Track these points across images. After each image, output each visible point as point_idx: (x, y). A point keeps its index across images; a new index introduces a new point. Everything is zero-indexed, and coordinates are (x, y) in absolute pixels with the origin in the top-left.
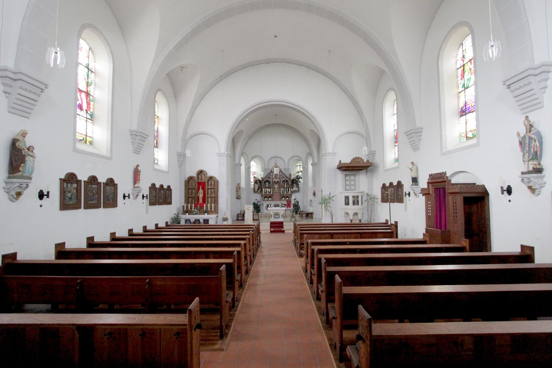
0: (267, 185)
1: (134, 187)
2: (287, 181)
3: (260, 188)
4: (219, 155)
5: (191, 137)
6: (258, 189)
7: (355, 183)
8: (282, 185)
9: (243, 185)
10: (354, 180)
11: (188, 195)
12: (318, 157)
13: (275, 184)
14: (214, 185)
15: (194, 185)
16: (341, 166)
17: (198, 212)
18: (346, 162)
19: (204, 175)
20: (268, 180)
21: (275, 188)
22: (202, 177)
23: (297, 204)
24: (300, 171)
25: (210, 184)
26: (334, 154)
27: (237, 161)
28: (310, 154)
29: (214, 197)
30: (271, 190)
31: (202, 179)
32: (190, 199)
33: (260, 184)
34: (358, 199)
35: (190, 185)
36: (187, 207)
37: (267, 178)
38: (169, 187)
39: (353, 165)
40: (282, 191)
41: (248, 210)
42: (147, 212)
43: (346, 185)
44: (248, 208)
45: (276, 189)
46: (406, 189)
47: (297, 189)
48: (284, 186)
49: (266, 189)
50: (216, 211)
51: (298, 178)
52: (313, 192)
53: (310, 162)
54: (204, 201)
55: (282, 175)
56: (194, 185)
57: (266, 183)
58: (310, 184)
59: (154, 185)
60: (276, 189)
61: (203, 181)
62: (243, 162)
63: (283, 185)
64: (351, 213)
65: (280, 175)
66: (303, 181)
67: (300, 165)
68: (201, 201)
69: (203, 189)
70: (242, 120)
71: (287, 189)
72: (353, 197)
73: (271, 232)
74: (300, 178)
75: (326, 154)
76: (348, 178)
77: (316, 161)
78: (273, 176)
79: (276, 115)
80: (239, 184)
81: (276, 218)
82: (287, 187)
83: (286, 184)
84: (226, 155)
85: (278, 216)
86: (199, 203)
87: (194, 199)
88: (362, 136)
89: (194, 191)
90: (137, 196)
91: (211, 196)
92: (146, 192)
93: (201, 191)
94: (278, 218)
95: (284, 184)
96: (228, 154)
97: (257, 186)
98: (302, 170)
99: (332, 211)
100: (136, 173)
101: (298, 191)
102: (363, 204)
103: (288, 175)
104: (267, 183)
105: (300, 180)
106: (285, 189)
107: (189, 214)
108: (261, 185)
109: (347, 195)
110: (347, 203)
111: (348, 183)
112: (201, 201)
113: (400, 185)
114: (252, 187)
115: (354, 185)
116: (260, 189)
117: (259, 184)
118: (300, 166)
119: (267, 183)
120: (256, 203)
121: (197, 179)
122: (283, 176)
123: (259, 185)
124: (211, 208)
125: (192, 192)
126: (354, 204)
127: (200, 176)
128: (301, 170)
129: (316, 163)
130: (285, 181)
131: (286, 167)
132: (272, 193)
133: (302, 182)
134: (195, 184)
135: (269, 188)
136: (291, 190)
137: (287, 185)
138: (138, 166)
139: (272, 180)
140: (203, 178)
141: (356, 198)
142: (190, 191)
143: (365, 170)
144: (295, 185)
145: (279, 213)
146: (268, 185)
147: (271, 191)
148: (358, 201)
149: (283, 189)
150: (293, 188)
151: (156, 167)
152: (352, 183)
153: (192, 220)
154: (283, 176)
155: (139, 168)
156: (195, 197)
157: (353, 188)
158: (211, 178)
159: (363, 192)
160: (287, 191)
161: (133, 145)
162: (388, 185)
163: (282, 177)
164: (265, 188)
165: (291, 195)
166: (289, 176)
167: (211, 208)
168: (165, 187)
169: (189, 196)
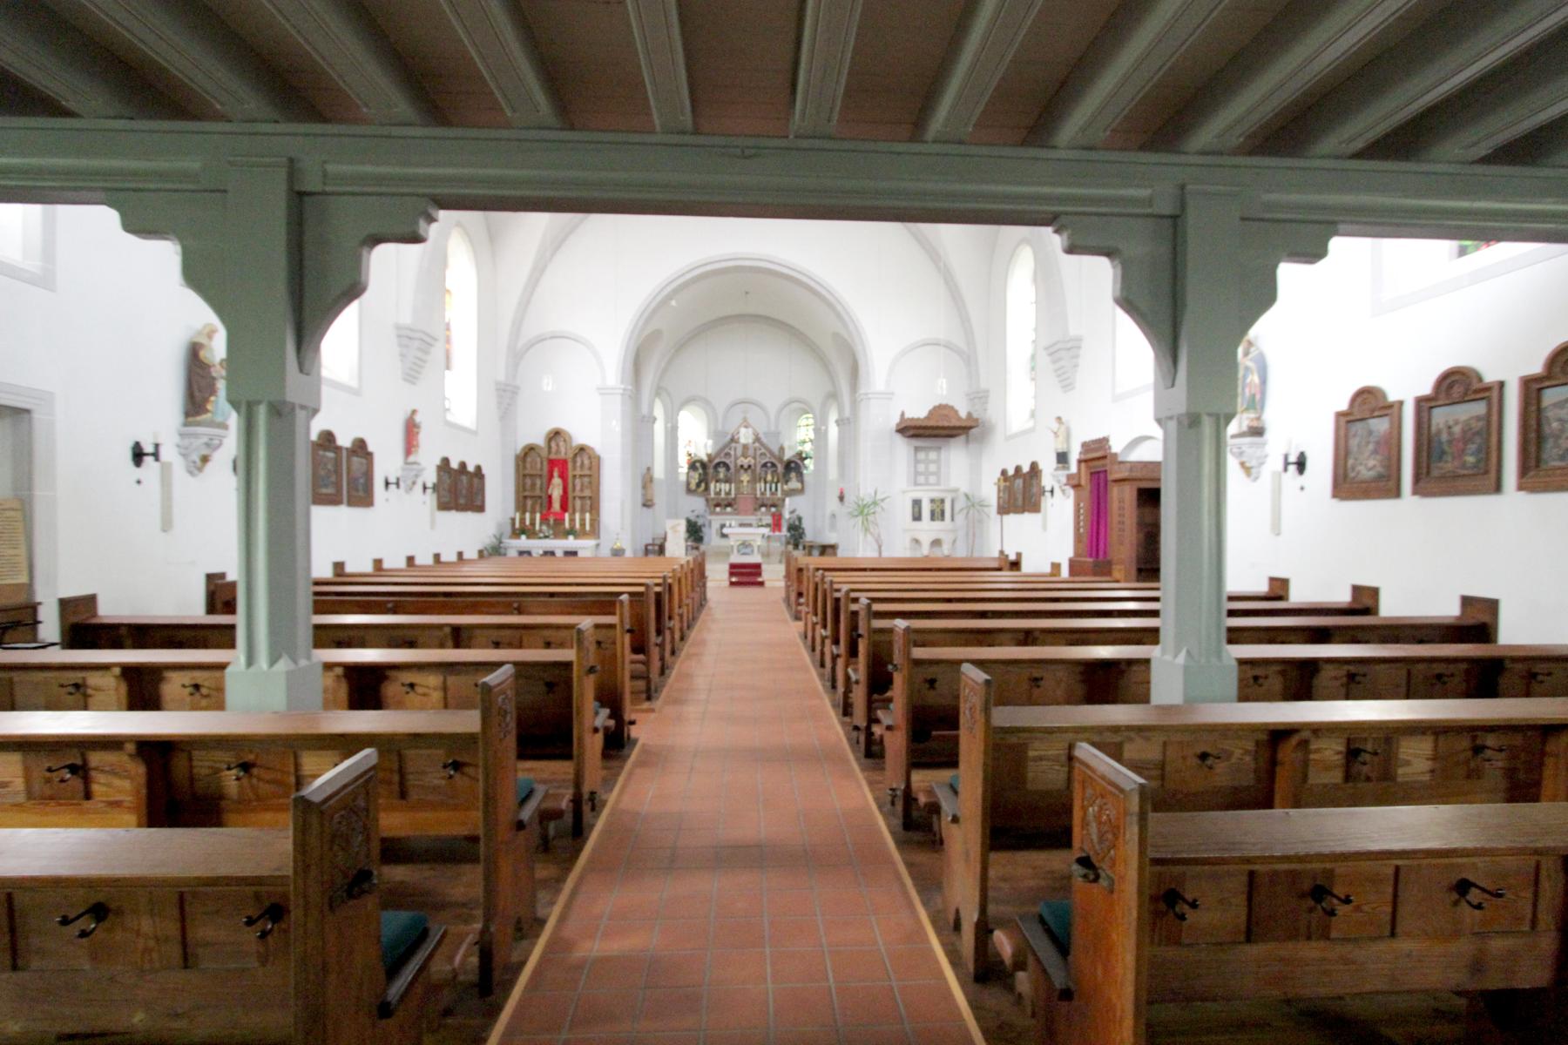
1: (406, 463)
2: (773, 465)
3: (704, 480)
4: (603, 391)
5: (531, 345)
6: (698, 485)
7: (939, 468)
9: (659, 472)
10: (937, 461)
11: (525, 490)
12: (855, 404)
13: (742, 471)
14: (590, 468)
15: (539, 466)
16: (903, 425)
17: (551, 532)
18: (916, 417)
19: (565, 441)
20: (723, 460)
21: (742, 482)
22: (558, 445)
23: (797, 523)
25: (578, 464)
26: (888, 395)
27: (645, 410)
28: (833, 396)
29: (590, 498)
31: (558, 451)
32: (529, 502)
33: (705, 471)
34: (943, 506)
35: (528, 466)
36: (522, 520)
37: (722, 455)
38: (478, 468)
39: (932, 423)
40: (760, 489)
41: (676, 531)
42: (433, 524)
43: (917, 473)
44: (674, 528)
45: (745, 484)
46: (1047, 480)
47: (798, 485)
48: (766, 474)
49: (718, 484)
50: (595, 532)
51: (801, 457)
52: (838, 494)
53: (833, 416)
54: (564, 507)
56: (538, 466)
58: (833, 472)
59: (446, 461)
60: (745, 484)
61: (562, 456)
62: (659, 412)
63: (763, 475)
64: (926, 540)
65: (755, 450)
66: (816, 465)
68: (556, 506)
69: (563, 476)
70: (659, 306)
71: (774, 486)
72: (932, 501)
73: (732, 584)
74: (806, 458)
75: (870, 396)
76: (922, 455)
77: (847, 413)
79: (747, 293)
80: (649, 469)
83: (769, 472)
84: (621, 391)
85: (748, 550)
86: (552, 510)
87: (539, 501)
88: (959, 352)
89: (538, 482)
90: (414, 483)
91: (582, 495)
92: (431, 477)
93: (557, 481)
96: (624, 390)
97: (695, 477)
99: (879, 535)
100: (411, 430)
101: (801, 491)
102: (956, 517)
103: (776, 450)
104: (722, 470)
105: (807, 462)
107: (528, 537)
108: (705, 474)
109: (917, 495)
110: (917, 517)
111: (921, 467)
112: (556, 506)
113: (1035, 470)
114: (683, 478)
115: (937, 474)
117: (701, 471)
118: (807, 425)
119: (722, 470)
120: (693, 518)
121: (546, 449)
123: (700, 474)
124: (583, 524)
125: (533, 485)
126: (933, 518)
127: (553, 445)
129: (848, 419)
130: (769, 465)
133: (811, 467)
134: (542, 463)
135: (727, 481)
138: (414, 412)
140: (563, 450)
141: (938, 503)
142: (528, 481)
143: (963, 438)
144: (793, 475)
145: (752, 543)
147: (730, 490)
148: (943, 513)
151: (449, 417)
152: (933, 468)
153: (537, 552)
154: (763, 451)
155: (418, 418)
156: (540, 497)
157: (932, 479)
158: (582, 449)
159: (956, 490)
161: (402, 361)
162: (1011, 472)
163: (761, 454)
164: (717, 481)
165: (784, 500)
166: (780, 452)
167: (583, 524)
168: (471, 468)
169: (527, 494)
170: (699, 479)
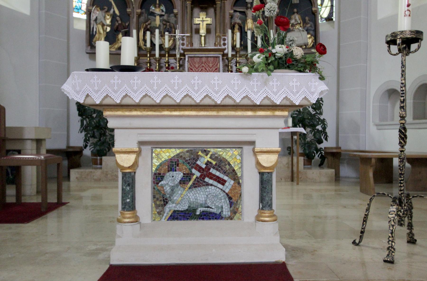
0: (158, 18)
8: (232, 17)
40: (234, 47)
48: (244, 21)
57: (152, 8)
95: (243, 13)
123: (114, 16)
144: (296, 18)
170: (112, 26)
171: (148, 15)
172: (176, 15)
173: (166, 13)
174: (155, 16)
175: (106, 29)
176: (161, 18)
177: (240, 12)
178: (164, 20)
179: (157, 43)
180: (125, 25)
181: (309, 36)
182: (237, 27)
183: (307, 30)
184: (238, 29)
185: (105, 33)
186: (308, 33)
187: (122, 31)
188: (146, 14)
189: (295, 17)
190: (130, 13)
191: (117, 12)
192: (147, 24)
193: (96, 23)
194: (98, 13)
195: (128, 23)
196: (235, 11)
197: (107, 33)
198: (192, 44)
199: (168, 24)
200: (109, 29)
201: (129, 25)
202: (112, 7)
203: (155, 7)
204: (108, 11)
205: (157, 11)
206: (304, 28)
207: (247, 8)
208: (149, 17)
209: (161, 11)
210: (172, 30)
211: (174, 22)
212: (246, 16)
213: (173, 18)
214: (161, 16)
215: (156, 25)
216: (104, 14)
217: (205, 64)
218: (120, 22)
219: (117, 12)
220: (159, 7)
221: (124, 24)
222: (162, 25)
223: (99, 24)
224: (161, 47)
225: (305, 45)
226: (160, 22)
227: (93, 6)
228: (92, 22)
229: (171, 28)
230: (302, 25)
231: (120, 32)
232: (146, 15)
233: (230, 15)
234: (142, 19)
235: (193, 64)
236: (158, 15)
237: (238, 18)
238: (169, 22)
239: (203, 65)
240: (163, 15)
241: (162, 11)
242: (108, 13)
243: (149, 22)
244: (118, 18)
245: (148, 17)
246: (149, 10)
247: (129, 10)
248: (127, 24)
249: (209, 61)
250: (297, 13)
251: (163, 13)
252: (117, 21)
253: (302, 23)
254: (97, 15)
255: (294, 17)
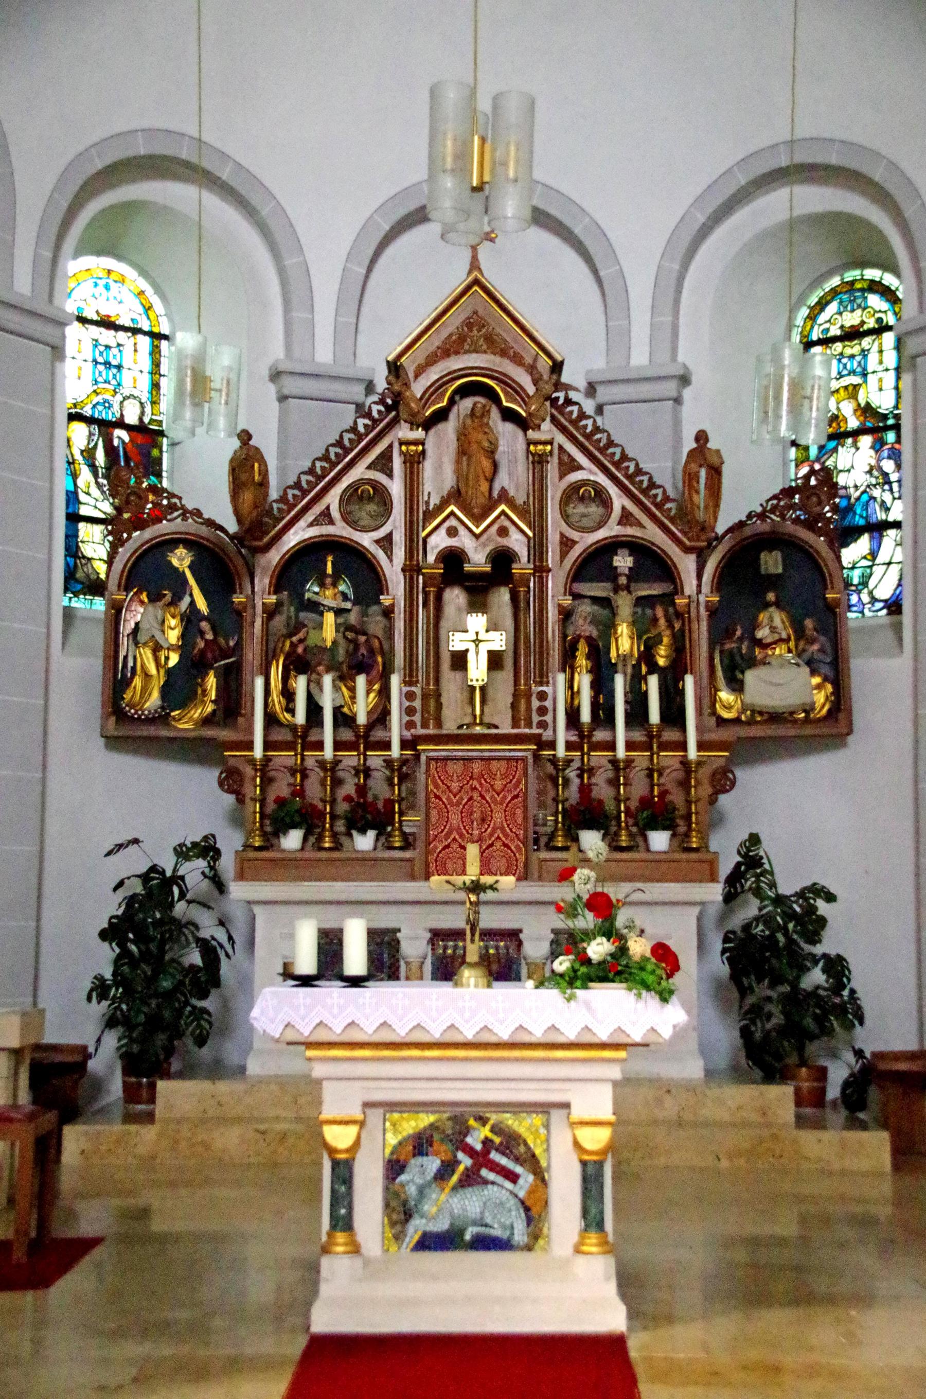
0: (329, 618)
13: (455, 597)
20: (340, 529)
21: (460, 661)
24: (853, 423)
30: (385, 693)
37: (333, 499)
40: (573, 715)
45: (477, 671)
48: (608, 628)
49: (300, 684)
55: (568, 465)
57: (312, 589)
60: (477, 671)
63: (583, 626)
65: (538, 462)
67: (851, 319)
71: (653, 684)
74: (849, 535)
78: (428, 468)
81: (428, 1243)
82: (647, 656)
83: (624, 604)
94: (485, 1243)
98: (884, 401)
106: (620, 684)
116: (211, 681)
118: (852, 334)
122: (589, 472)
123: (191, 619)
128: (867, 410)
130: (623, 562)
131: (640, 358)
132: (404, 744)
136: (707, 703)
137: (641, 628)
139: (399, 538)
145: (523, 1125)
146: (344, 628)
147: (381, 717)
149: (584, 681)
150: (750, 677)
154: (589, 472)
160: (654, 716)
163: (573, 494)
166: (690, 478)
171: (298, 610)
172: (388, 613)
173: (354, 605)
174: (321, 614)
175: (167, 658)
176: (340, 620)
177: (595, 600)
178: (350, 628)
179: (327, 702)
180: (227, 644)
181: (816, 680)
182: (583, 649)
183: (809, 663)
184: (588, 657)
185: (162, 672)
186: (813, 673)
187: (216, 665)
188: (291, 605)
189: (771, 619)
190: (240, 607)
191: (202, 605)
192: (295, 639)
193: (136, 643)
194: (141, 610)
195: (236, 638)
196: (576, 596)
197: (169, 672)
198: (439, 724)
199: (362, 639)
200: (174, 659)
201: (239, 645)
202: (188, 593)
203: (322, 585)
204: (174, 602)
205: (328, 598)
206: (799, 655)
207: (617, 589)
208: (302, 615)
209: (339, 597)
210: (376, 661)
211: (380, 634)
212: (614, 614)
213: (379, 618)
214: (339, 612)
215: (324, 641)
216: (160, 613)
217: (481, 784)
218: (210, 636)
219: (202, 605)
220: (334, 585)
221: (221, 641)
222: (342, 641)
223: (145, 644)
224: (343, 719)
225: (805, 711)
226: (337, 631)
227: (127, 589)
228: (124, 642)
229: (372, 652)
230: (792, 644)
231: (211, 668)
232: (292, 609)
233: (560, 613)
234: (279, 622)
235: (442, 781)
236: (330, 609)
237: (588, 620)
238: (365, 633)
239: (475, 783)
240: (348, 611)
241: (345, 597)
242: (172, 609)
243: (301, 635)
244: (204, 625)
245: (297, 617)
246: (303, 596)
247: (238, 599)
248: (232, 643)
249: (494, 770)
250: (777, 604)
251: (348, 605)
252: (202, 633)
253: (792, 638)
254: (139, 618)
255: (765, 621)
